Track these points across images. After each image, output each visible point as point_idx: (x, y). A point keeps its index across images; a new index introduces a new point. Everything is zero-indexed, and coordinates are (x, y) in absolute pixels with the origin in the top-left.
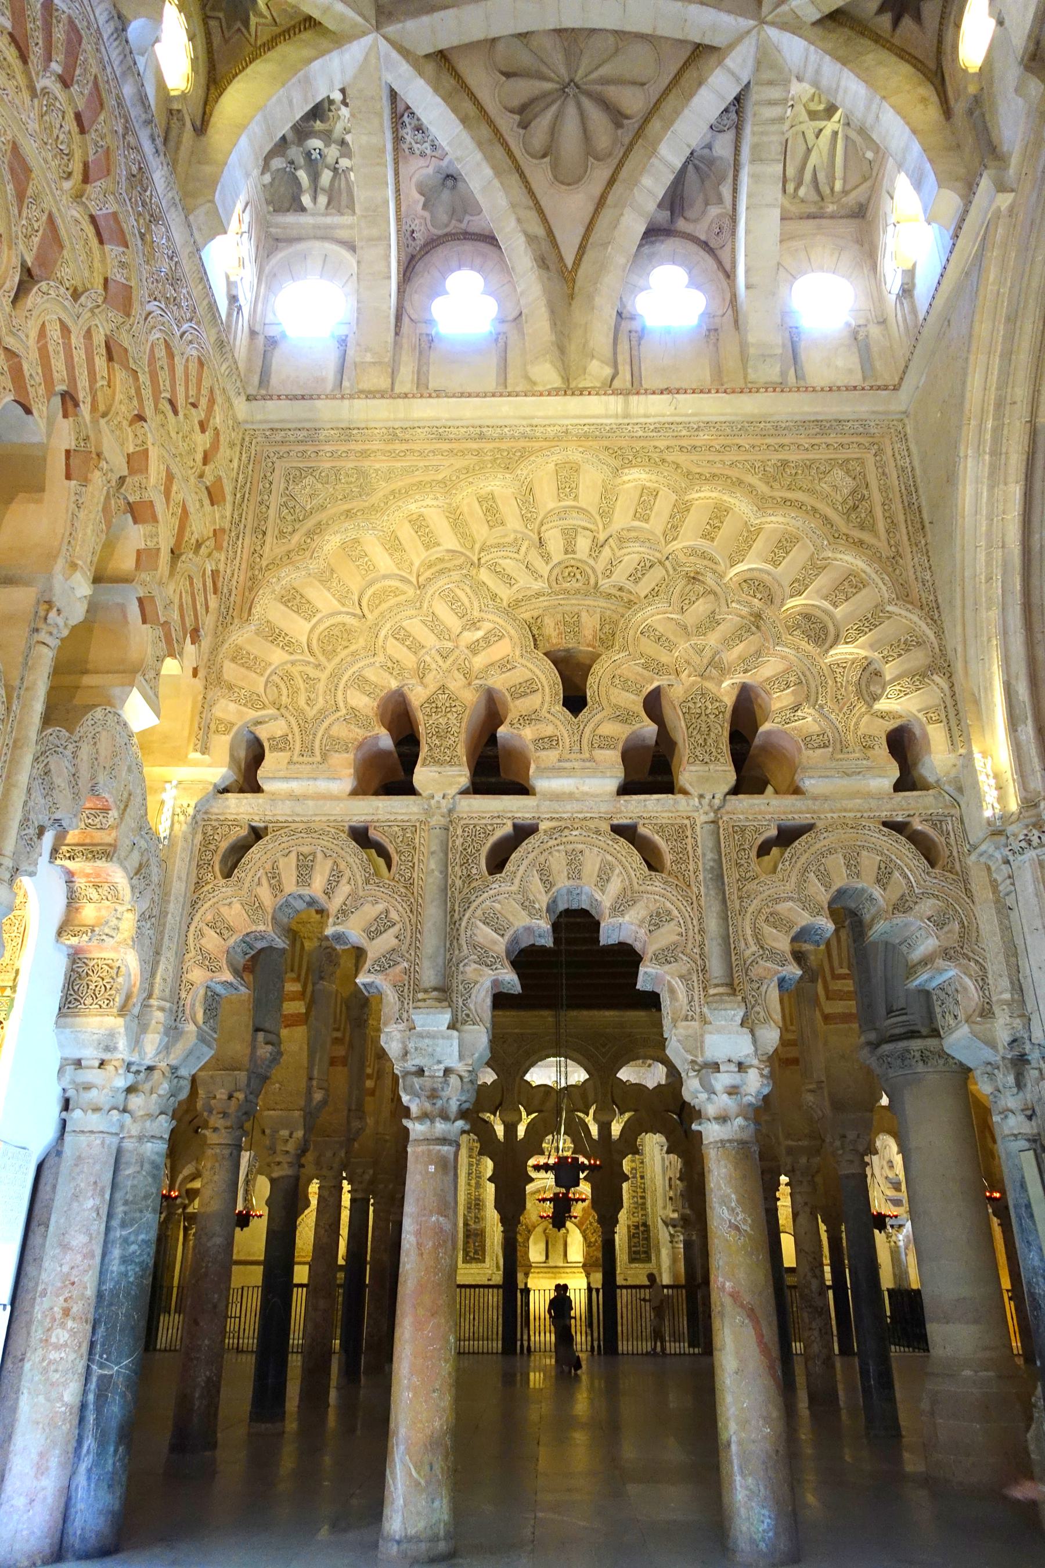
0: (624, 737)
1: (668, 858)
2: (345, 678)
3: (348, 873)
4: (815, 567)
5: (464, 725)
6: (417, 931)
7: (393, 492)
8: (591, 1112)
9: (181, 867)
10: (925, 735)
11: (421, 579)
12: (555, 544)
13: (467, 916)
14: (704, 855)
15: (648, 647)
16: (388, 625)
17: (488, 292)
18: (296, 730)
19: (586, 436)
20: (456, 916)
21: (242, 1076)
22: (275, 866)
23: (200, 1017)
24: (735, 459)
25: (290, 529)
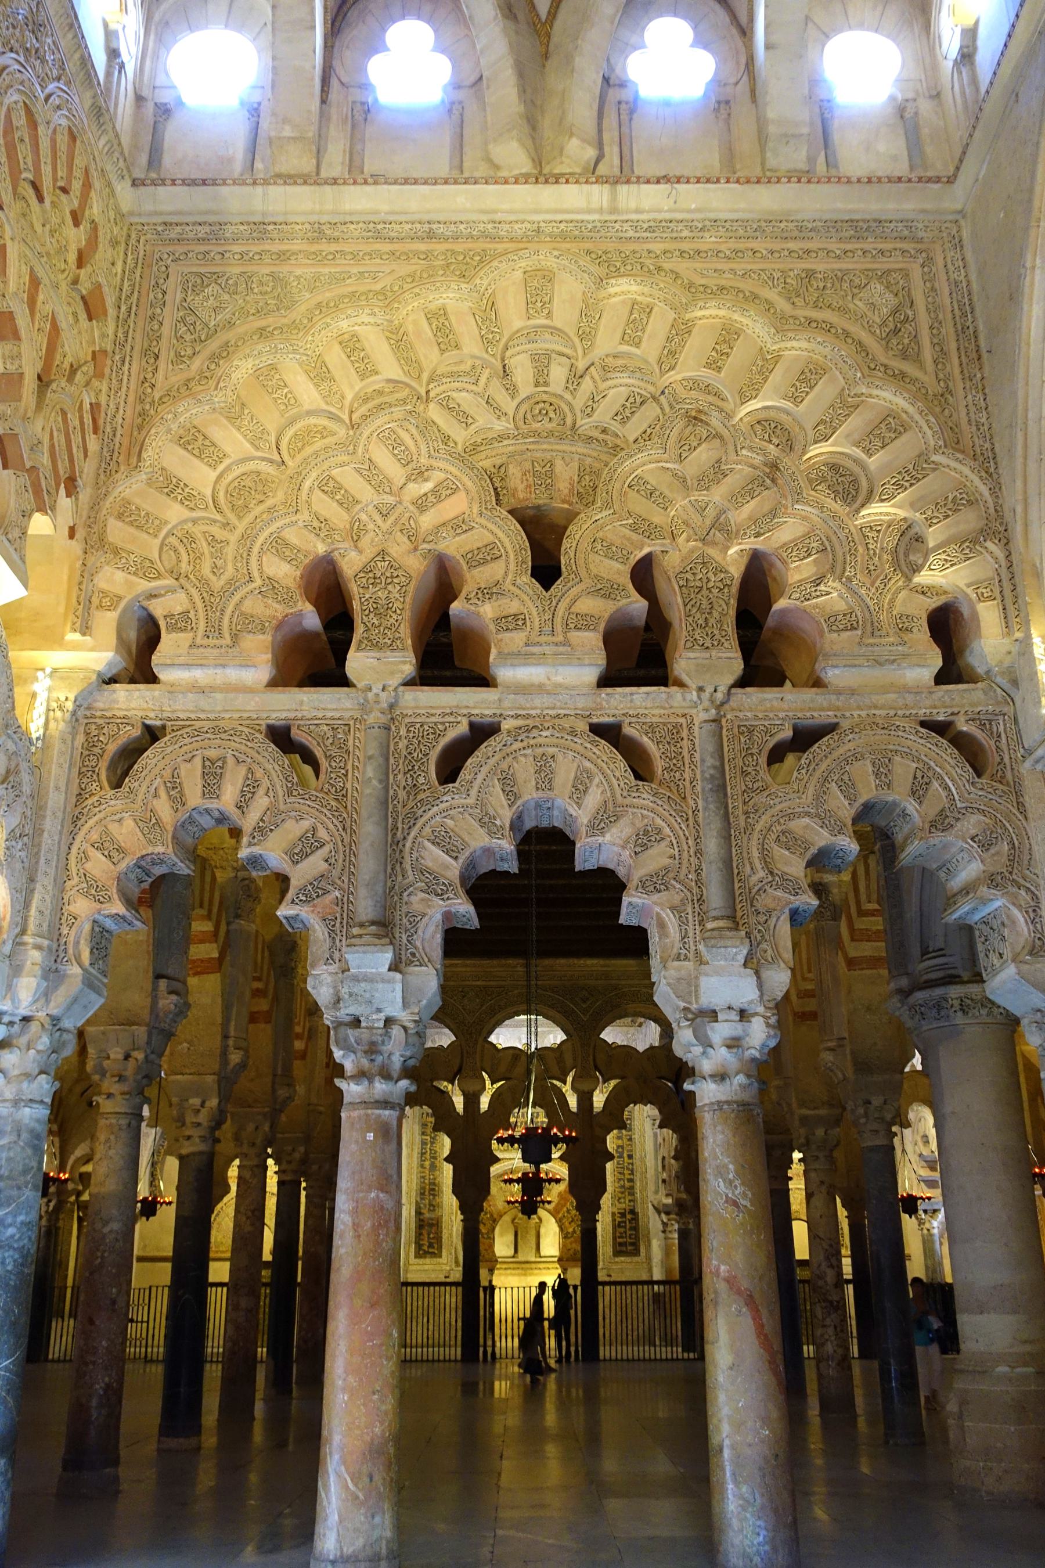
0: (606, 616)
1: (659, 764)
2: (261, 540)
3: (265, 783)
5: (408, 599)
6: (351, 852)
7: (319, 305)
8: (569, 1079)
10: (975, 616)
11: (354, 417)
12: (523, 373)
13: (412, 834)
14: (703, 761)
15: (638, 504)
16: (314, 475)
17: (440, 47)
18: (200, 605)
19: (564, 237)
20: (399, 835)
21: (141, 1032)
22: (175, 773)
23: (86, 956)
24: (749, 267)
25: (189, 351)
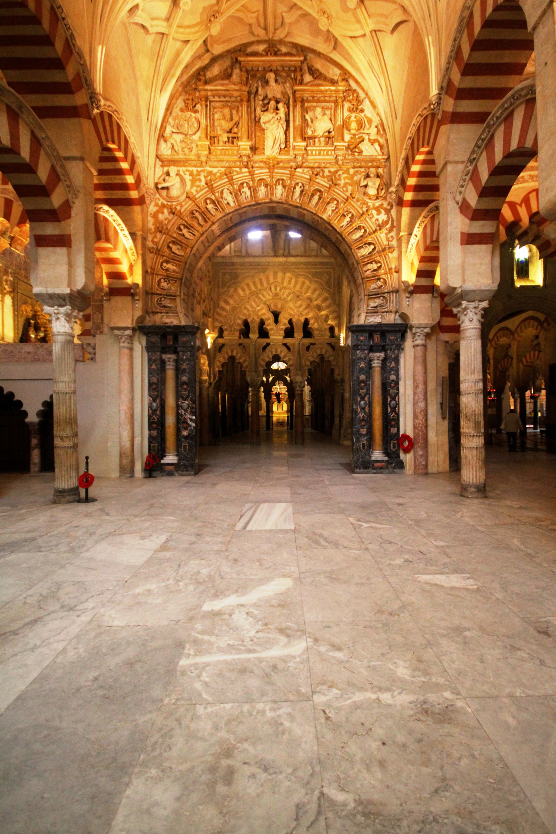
4: (320, 295)
9: (212, 351)
12: (273, 289)
15: (289, 311)
